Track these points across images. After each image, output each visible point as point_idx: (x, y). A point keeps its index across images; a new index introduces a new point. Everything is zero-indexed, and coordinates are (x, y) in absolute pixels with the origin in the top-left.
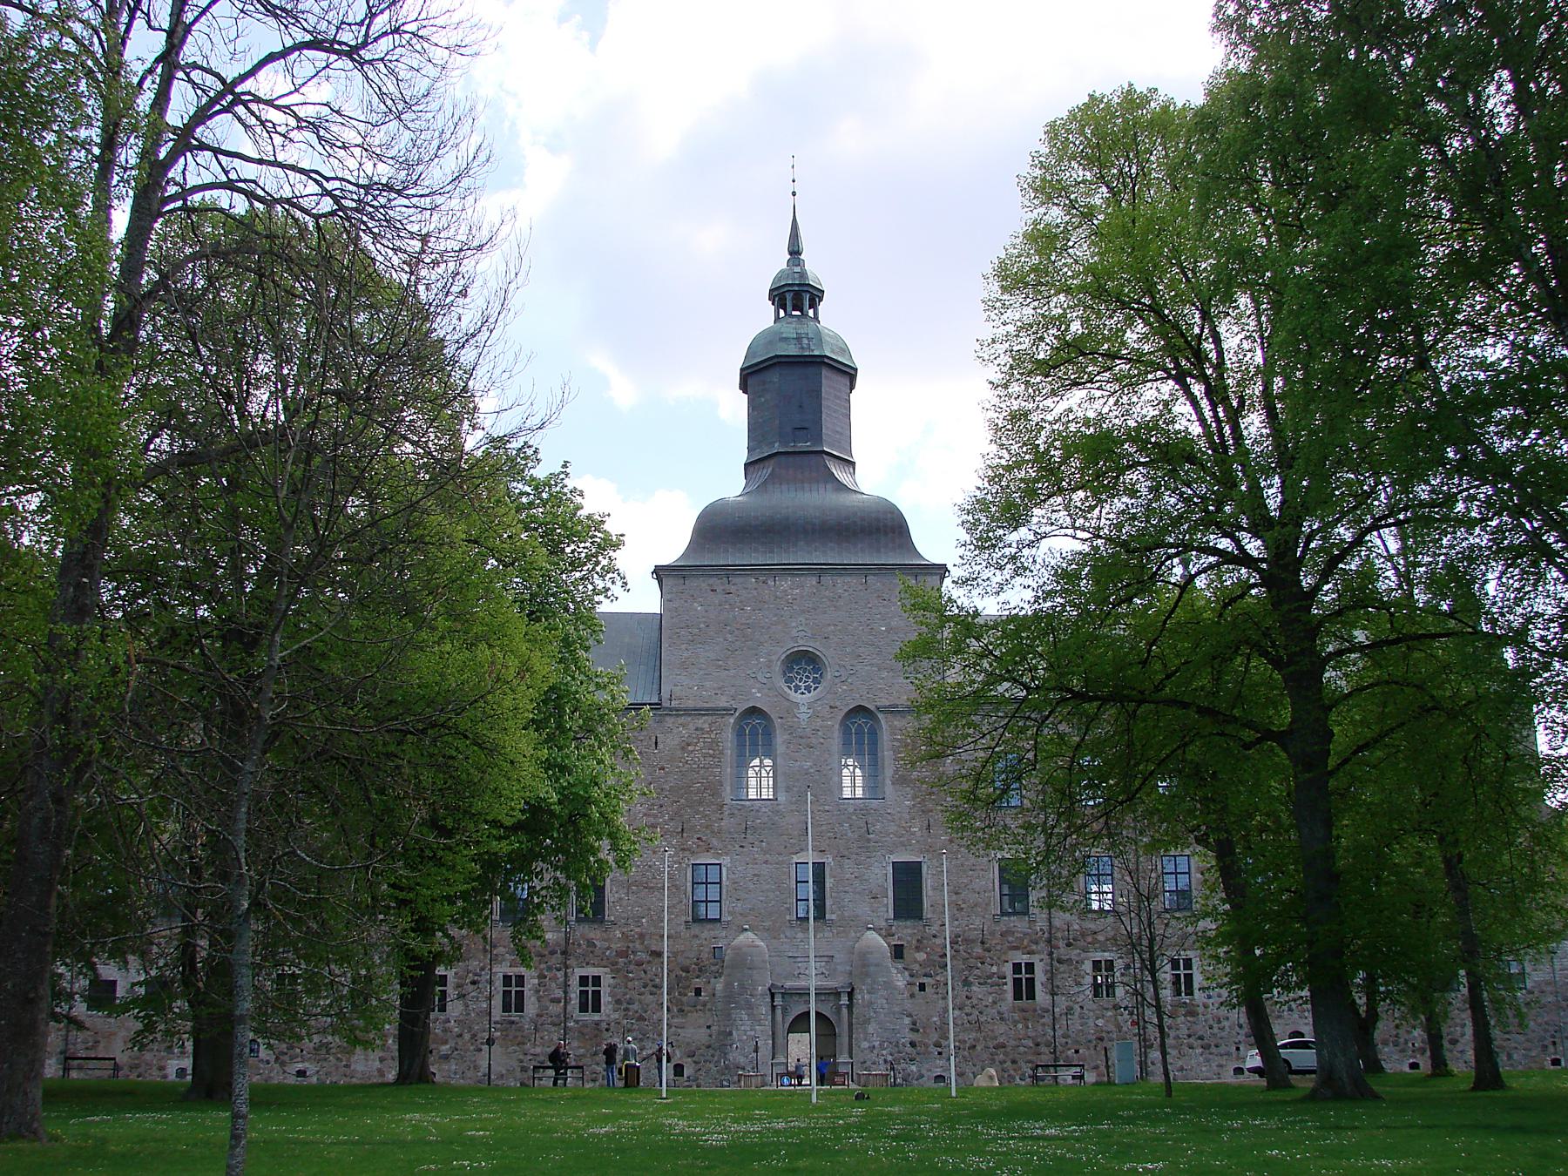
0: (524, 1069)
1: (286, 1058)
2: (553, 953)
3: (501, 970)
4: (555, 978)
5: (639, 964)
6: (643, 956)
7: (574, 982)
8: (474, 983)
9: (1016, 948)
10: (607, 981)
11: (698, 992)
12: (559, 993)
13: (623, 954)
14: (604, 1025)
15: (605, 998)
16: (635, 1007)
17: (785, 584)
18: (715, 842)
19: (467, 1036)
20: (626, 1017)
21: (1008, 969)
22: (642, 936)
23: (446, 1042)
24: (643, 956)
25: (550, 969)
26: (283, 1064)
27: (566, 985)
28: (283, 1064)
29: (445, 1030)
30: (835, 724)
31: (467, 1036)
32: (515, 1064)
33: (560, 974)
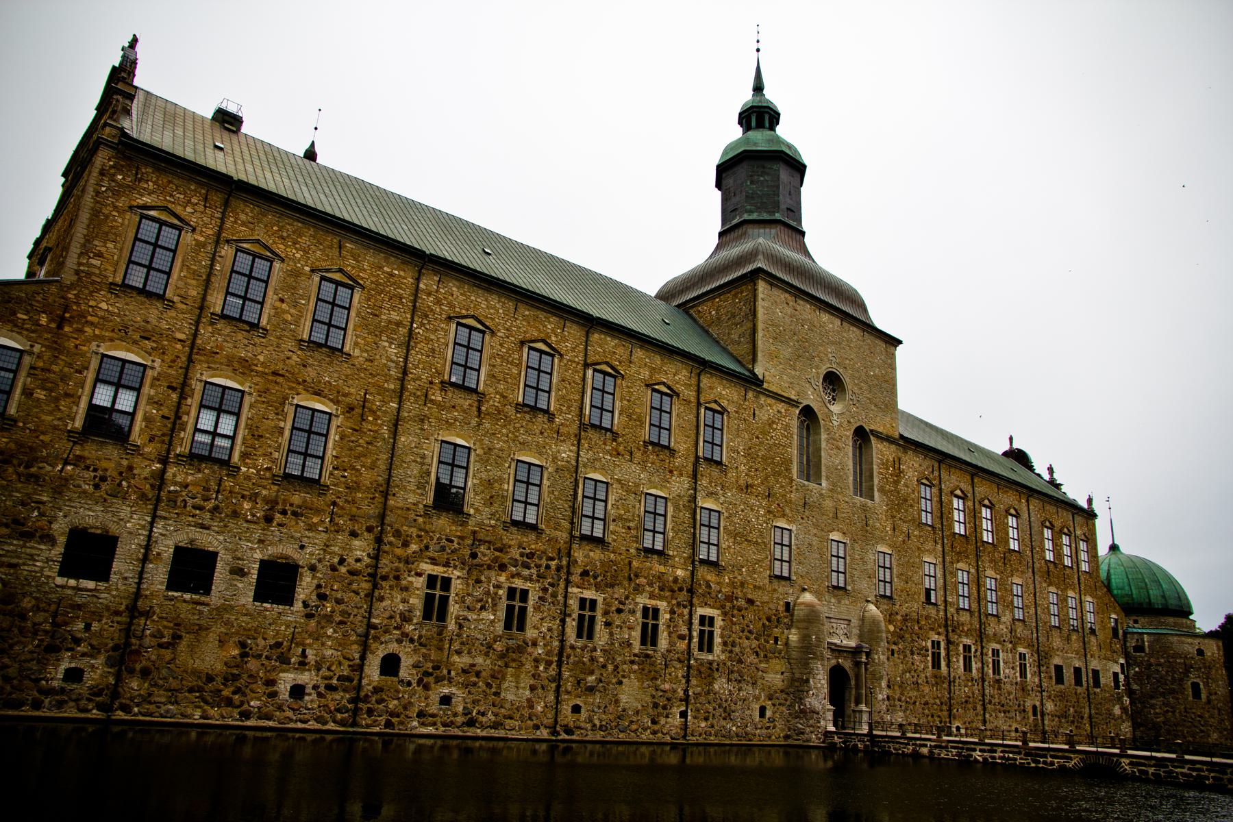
0: (656, 705)
1: (431, 679)
2: (681, 589)
3: (642, 600)
4: (682, 615)
5: (740, 610)
6: (742, 603)
7: (696, 621)
8: (619, 611)
9: (932, 629)
10: (719, 622)
11: (776, 639)
12: (684, 630)
13: (730, 598)
14: (715, 665)
15: (717, 640)
16: (737, 649)
17: (825, 317)
18: (787, 511)
19: (610, 667)
20: (730, 659)
21: (929, 644)
22: (742, 584)
23: (592, 673)
24: (742, 603)
25: (678, 604)
26: (426, 687)
27: (691, 624)
28: (426, 687)
29: (592, 659)
30: (850, 433)
31: (610, 667)
32: (648, 699)
33: (686, 611)
